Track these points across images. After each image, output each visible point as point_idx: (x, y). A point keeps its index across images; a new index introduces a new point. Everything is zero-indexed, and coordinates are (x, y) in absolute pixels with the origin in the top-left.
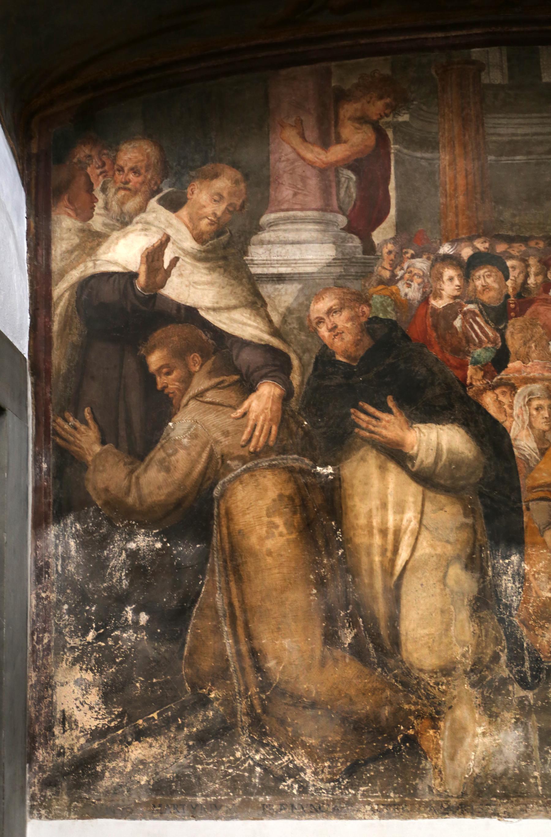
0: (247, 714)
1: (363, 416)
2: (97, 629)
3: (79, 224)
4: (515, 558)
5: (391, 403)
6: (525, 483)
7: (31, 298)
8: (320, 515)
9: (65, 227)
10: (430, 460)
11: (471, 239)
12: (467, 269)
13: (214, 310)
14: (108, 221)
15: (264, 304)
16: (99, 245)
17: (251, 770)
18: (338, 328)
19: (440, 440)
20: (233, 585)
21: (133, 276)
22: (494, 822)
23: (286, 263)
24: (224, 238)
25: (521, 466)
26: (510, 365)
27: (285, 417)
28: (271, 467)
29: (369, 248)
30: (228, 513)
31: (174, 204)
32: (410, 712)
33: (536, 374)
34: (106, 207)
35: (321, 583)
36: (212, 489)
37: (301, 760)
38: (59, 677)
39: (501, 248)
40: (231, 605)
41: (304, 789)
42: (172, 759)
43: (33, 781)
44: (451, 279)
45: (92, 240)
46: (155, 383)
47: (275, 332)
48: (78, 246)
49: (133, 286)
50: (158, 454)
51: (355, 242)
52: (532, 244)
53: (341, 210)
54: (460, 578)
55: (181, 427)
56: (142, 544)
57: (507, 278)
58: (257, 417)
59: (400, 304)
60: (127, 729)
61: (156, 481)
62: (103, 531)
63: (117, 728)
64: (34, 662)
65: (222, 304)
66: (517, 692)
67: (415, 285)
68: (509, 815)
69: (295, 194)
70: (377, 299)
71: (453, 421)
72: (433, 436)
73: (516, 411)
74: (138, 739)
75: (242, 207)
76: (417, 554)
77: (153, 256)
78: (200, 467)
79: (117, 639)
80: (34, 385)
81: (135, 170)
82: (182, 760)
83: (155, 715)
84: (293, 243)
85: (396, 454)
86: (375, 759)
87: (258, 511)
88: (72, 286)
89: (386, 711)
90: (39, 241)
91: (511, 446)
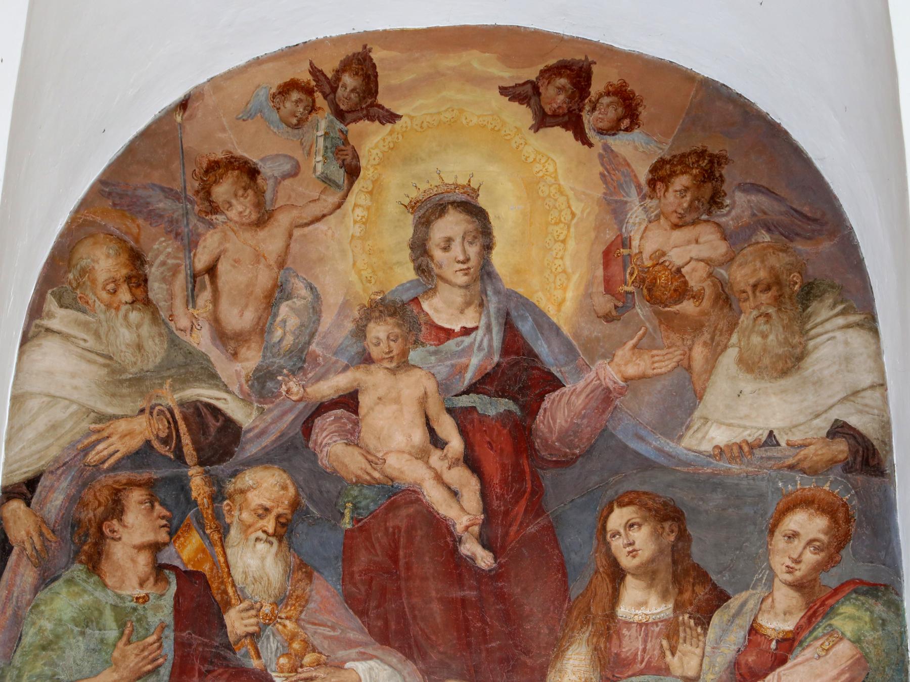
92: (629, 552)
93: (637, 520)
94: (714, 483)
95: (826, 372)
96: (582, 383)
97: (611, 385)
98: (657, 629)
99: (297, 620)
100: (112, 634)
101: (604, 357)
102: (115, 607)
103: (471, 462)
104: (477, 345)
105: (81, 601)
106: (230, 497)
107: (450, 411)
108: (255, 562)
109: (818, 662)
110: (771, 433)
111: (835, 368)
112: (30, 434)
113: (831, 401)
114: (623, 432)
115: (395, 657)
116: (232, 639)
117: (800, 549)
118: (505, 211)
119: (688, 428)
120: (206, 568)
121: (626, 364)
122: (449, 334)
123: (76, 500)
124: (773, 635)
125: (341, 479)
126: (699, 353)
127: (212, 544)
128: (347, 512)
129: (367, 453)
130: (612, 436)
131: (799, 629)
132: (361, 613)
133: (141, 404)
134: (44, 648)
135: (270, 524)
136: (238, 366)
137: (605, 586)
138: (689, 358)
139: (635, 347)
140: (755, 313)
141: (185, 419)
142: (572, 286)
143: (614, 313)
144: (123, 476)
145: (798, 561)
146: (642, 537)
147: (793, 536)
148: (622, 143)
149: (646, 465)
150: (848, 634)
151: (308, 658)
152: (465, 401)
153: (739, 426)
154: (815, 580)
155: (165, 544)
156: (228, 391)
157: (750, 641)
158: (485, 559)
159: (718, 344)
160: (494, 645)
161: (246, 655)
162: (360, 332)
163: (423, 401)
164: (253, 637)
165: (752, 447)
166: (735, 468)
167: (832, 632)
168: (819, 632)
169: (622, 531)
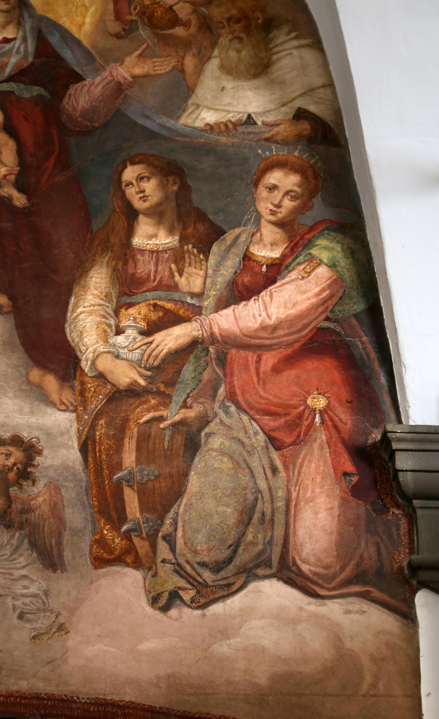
92: (141, 198)
93: (147, 174)
95: (288, 76)
96: (98, 79)
97: (122, 81)
98: (167, 256)
101: (116, 61)
104: (15, 49)
109: (302, 282)
110: (249, 116)
111: (294, 73)
113: (294, 95)
114: (133, 112)
117: (279, 198)
119: (184, 111)
121: (133, 67)
124: (264, 261)
126: (189, 62)
130: (124, 115)
131: (284, 256)
137: (121, 222)
138: (182, 64)
139: (140, 56)
140: (230, 36)
142: (89, 14)
143: (123, 33)
145: (279, 206)
146: (150, 186)
147: (273, 188)
149: (151, 135)
150: (325, 261)
153: (224, 111)
154: (294, 220)
157: (244, 265)
158: (19, 200)
159: (204, 56)
160: (26, 265)
165: (235, 125)
166: (223, 139)
167: (311, 258)
169: (134, 182)
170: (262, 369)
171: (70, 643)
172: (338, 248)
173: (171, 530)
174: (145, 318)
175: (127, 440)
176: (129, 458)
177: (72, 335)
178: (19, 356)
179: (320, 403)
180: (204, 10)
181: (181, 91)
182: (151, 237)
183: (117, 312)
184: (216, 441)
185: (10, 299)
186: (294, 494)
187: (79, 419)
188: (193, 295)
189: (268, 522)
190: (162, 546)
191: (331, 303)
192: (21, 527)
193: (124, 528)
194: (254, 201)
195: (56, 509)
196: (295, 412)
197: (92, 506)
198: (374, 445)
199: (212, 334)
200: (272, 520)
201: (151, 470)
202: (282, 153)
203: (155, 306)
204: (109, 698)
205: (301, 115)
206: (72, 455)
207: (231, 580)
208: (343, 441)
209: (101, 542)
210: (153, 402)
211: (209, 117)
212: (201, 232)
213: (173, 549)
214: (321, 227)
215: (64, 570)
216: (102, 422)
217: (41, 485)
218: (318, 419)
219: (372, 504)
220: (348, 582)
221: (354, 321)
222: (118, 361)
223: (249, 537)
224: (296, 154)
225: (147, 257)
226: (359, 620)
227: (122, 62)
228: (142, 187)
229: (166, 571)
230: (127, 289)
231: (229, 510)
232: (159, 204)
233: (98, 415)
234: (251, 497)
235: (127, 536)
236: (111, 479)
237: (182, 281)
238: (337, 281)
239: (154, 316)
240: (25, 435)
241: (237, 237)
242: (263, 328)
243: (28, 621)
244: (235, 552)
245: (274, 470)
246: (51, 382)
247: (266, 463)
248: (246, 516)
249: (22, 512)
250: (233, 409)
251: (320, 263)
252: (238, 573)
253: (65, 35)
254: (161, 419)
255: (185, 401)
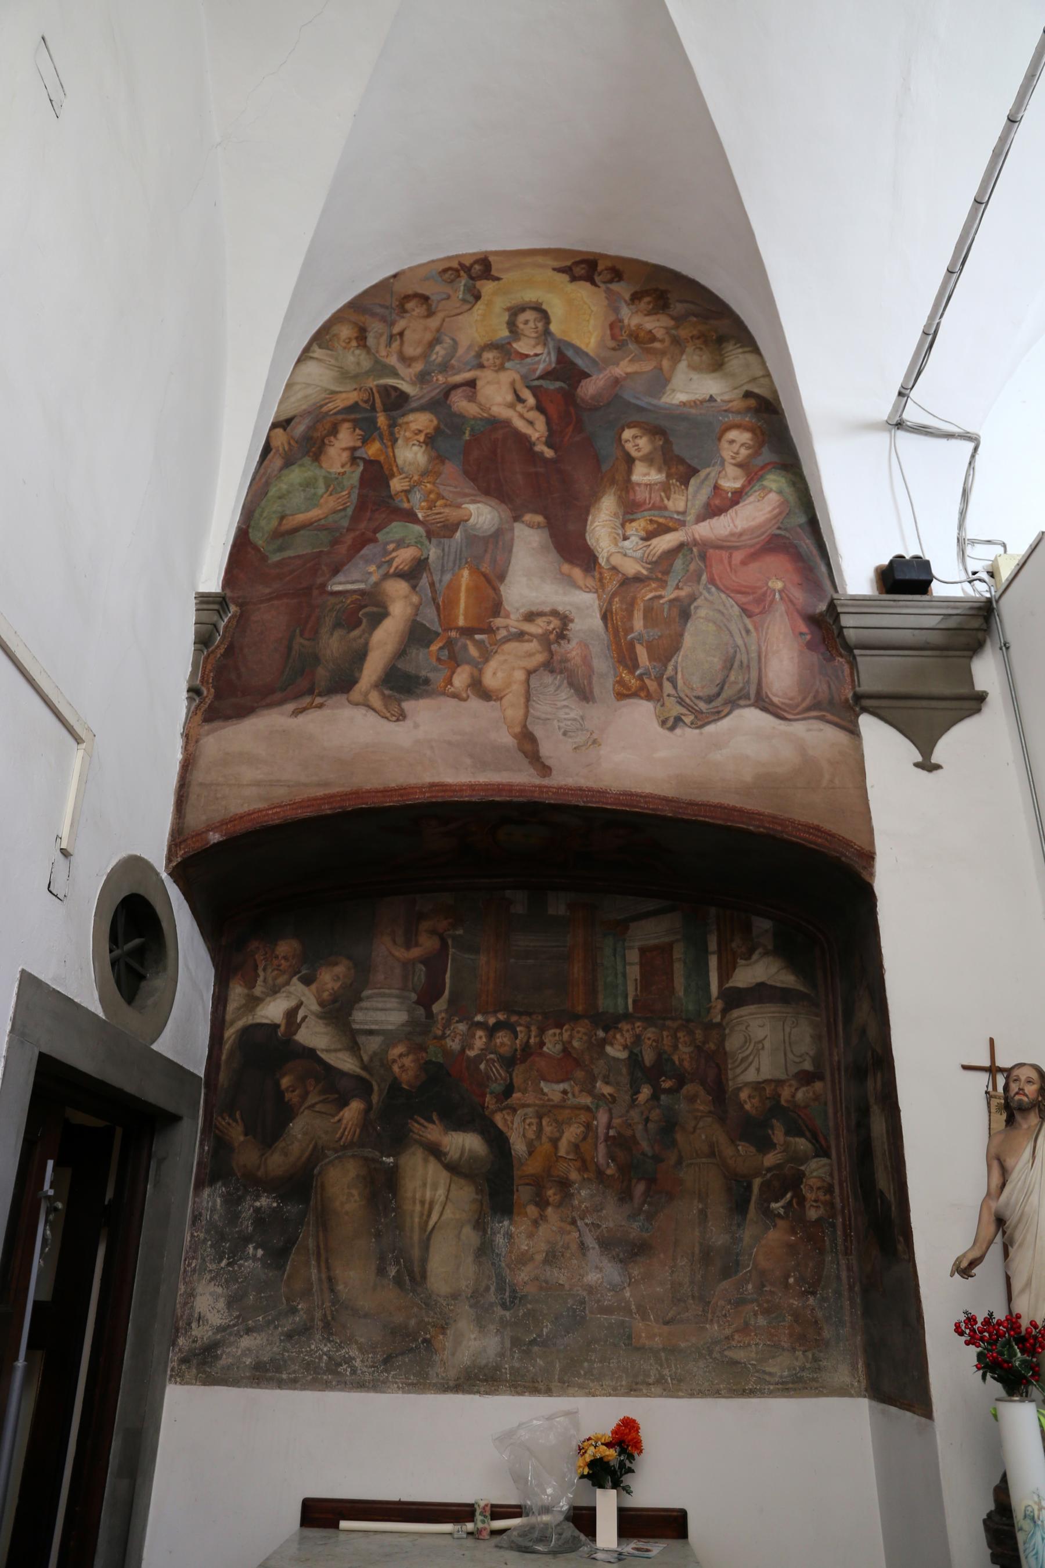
0: (321, 1320)
1: (416, 1125)
2: (228, 1259)
3: (246, 991)
4: (506, 1223)
5: (435, 1117)
6: (517, 1173)
7: (210, 1037)
8: (383, 1189)
9: (237, 992)
10: (456, 1156)
11: (495, 1012)
12: (491, 1031)
13: (327, 1051)
14: (264, 990)
15: (359, 1049)
16: (257, 1005)
17: (320, 1358)
18: (405, 1066)
19: (465, 1143)
20: (321, 1234)
21: (277, 1026)
22: (477, 1397)
23: (376, 1022)
24: (337, 1005)
25: (515, 1162)
26: (514, 1095)
27: (366, 1124)
28: (354, 1156)
29: (430, 1015)
30: (323, 1187)
31: (307, 981)
32: (429, 1323)
33: (530, 1101)
34: (265, 981)
35: (378, 1235)
36: (313, 1169)
37: (354, 1352)
38: (200, 1289)
39: (514, 1019)
40: (318, 1247)
41: (354, 1372)
42: (269, 1348)
43: (174, 1357)
44: (481, 1038)
45: (253, 1002)
46: (284, 1097)
47: (364, 1067)
48: (244, 1005)
49: (276, 1033)
50: (280, 1144)
51: (421, 1011)
52: (534, 1017)
53: (414, 990)
54: (470, 1236)
55: (297, 1127)
56: (264, 1203)
57: (516, 1038)
58: (347, 1124)
59: (447, 1053)
60: (241, 1327)
61: (277, 1162)
62: (240, 1193)
63: (234, 1325)
64: (184, 1279)
65: (332, 1047)
66: (499, 1311)
67: (457, 1040)
68: (487, 1393)
69: (386, 978)
70: (432, 1049)
71: (474, 1131)
72: (460, 1140)
73: (515, 1125)
74: (247, 1334)
75: (351, 985)
76: (443, 1218)
77: (291, 1014)
78: (307, 1154)
79: (240, 1266)
80: (206, 1095)
81: (285, 958)
82: (275, 1349)
83: (260, 1318)
84: (382, 1010)
85: (435, 1151)
86: (402, 1354)
87: (343, 1186)
88: (237, 1031)
89: (413, 1322)
90: (220, 1000)
91: (510, 1149)
94: (683, 418)
96: (601, 376)
99: (434, 484)
100: (321, 490)
102: (325, 478)
103: (540, 408)
105: (306, 475)
106: (400, 425)
107: (528, 387)
108: (411, 455)
110: (711, 396)
112: (293, 399)
114: (628, 396)
115: (494, 502)
116: (393, 493)
118: (556, 308)
119: (664, 393)
120: (382, 458)
122: (527, 356)
123: (312, 428)
125: (464, 417)
126: (666, 363)
127: (386, 447)
128: (467, 433)
129: (480, 405)
131: (743, 487)
132: (473, 480)
133: (355, 386)
134: (280, 498)
135: (422, 438)
136: (411, 370)
139: (630, 361)
141: (378, 392)
144: (340, 417)
145: (737, 453)
147: (732, 442)
148: (614, 286)
149: (641, 409)
151: (438, 503)
152: (536, 383)
155: (359, 447)
156: (403, 379)
158: (549, 453)
161: (401, 501)
162: (479, 355)
163: (513, 384)
164: (407, 492)
165: (702, 402)
166: (693, 411)
167: (764, 488)
168: (756, 488)
170: (733, 562)
171: (602, 752)
172: (783, 480)
173: (673, 673)
174: (644, 529)
175: (636, 612)
176: (638, 623)
177: (591, 541)
178: (553, 555)
179: (779, 585)
180: (673, 332)
181: (661, 382)
182: (644, 475)
183: (623, 525)
184: (702, 612)
185: (546, 517)
186: (764, 649)
187: (599, 598)
188: (678, 513)
189: (745, 668)
190: (668, 687)
191: (781, 517)
192: (561, 672)
193: (638, 672)
194: (718, 450)
195: (586, 660)
196: (760, 592)
197: (613, 658)
198: (821, 614)
199: (695, 540)
200: (748, 666)
201: (655, 632)
202: (737, 419)
203: (651, 521)
204: (633, 790)
205: (748, 395)
206: (597, 622)
207: (720, 709)
208: (798, 611)
209: (621, 682)
210: (654, 585)
211: (681, 397)
212: (682, 471)
213: (675, 687)
214: (769, 467)
215: (594, 702)
216: (617, 599)
217: (574, 643)
218: (777, 596)
219: (822, 654)
220: (809, 709)
221: (799, 530)
222: (626, 559)
223: (732, 678)
224: (747, 419)
225: (643, 487)
226: (818, 736)
227: (618, 364)
228: (636, 442)
229: (670, 702)
230: (629, 509)
231: (716, 660)
232: (650, 453)
233: (614, 595)
234: (731, 651)
235: (640, 678)
236: (625, 638)
237: (670, 504)
238: (785, 502)
239: (650, 528)
240: (560, 609)
241: (709, 474)
242: (732, 534)
243: (570, 737)
244: (722, 688)
245: (748, 632)
246: (577, 573)
247: (741, 626)
248: (729, 664)
249: (561, 662)
250: (713, 589)
251: (771, 491)
252: (726, 703)
253: (578, 350)
254: (661, 597)
255: (677, 585)
